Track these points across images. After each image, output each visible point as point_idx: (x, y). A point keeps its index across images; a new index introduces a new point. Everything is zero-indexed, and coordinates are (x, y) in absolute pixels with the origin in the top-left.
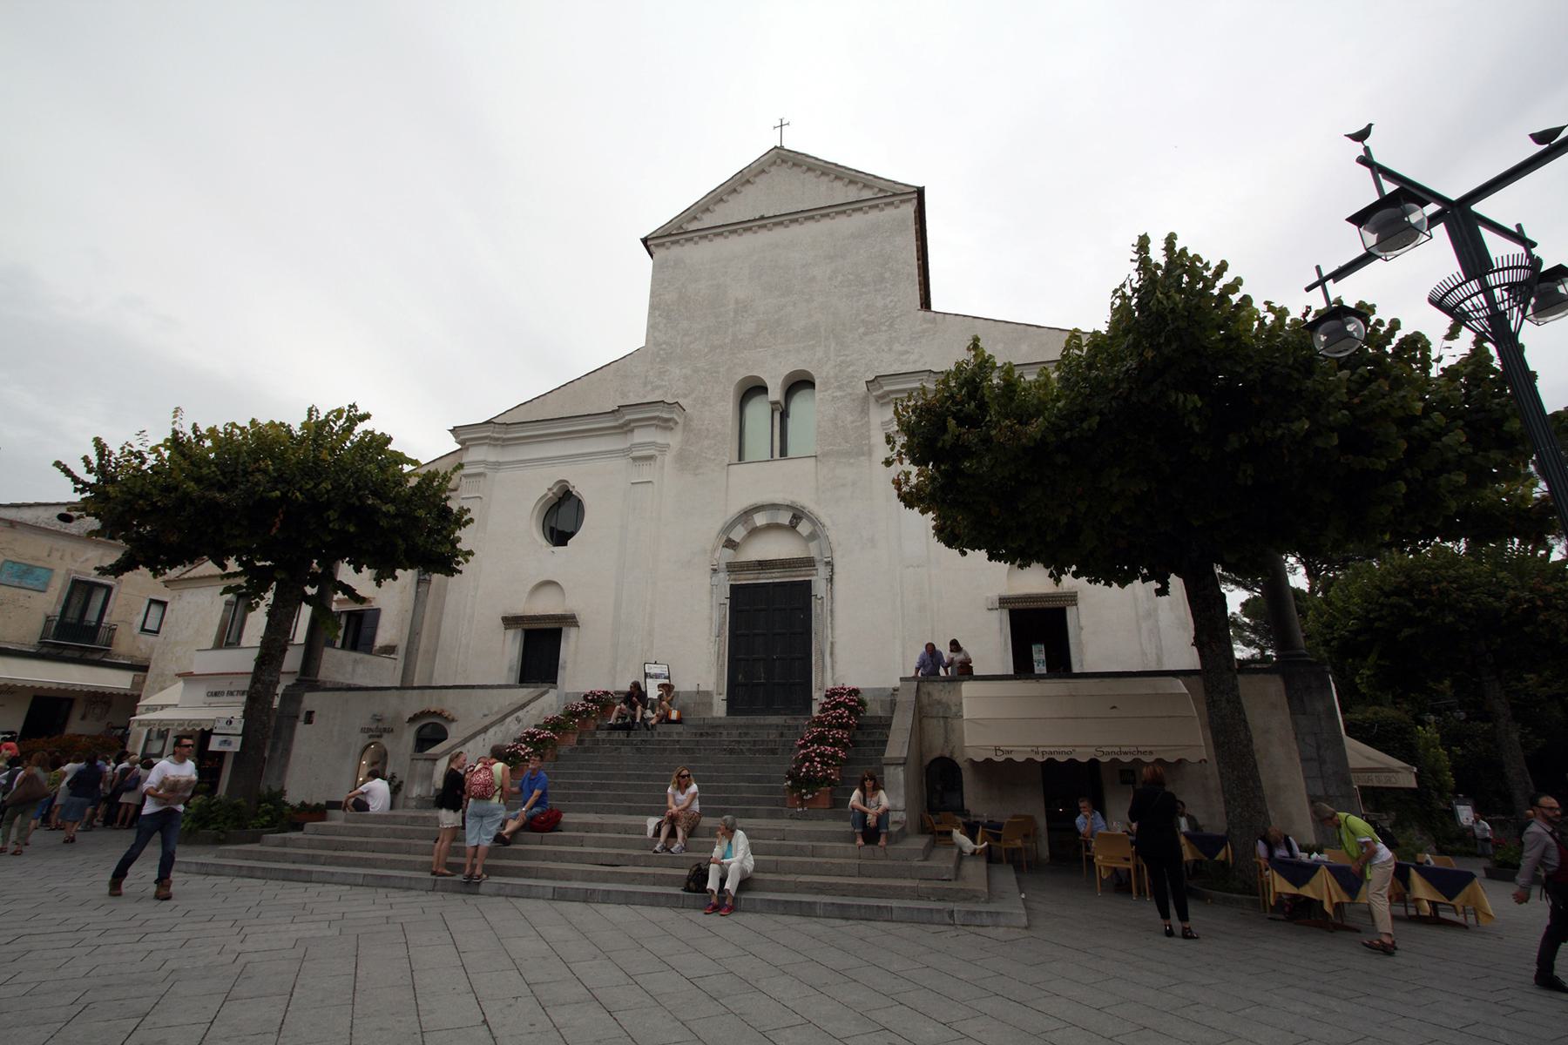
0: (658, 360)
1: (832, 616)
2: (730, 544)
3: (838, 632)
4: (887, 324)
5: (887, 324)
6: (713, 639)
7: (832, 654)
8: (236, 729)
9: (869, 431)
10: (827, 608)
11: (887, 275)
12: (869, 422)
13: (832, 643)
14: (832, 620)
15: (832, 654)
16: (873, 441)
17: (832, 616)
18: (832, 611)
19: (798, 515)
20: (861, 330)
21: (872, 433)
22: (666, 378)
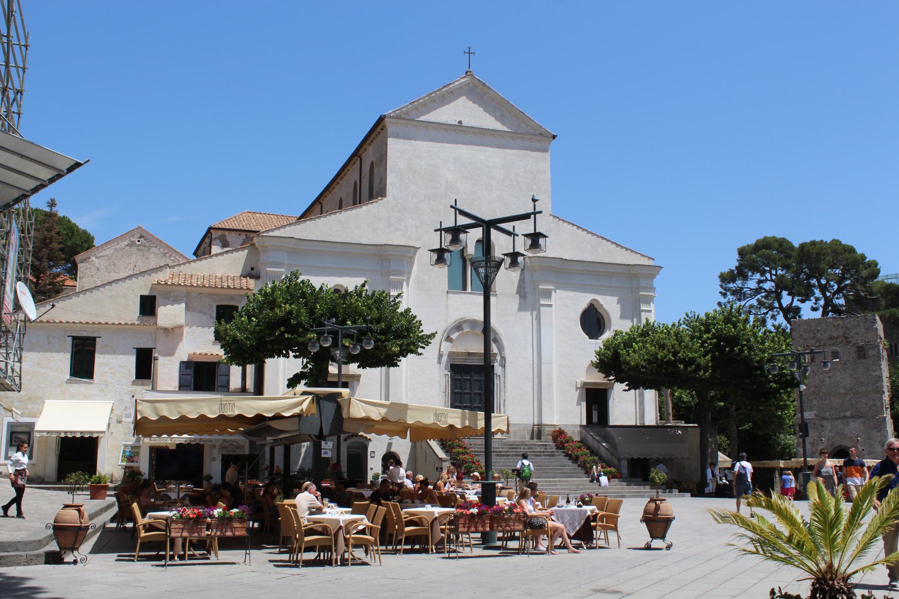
0: (397, 209)
1: (504, 385)
3: (507, 394)
6: (441, 394)
7: (504, 405)
8: (329, 446)
9: (524, 283)
10: (502, 381)
11: (534, 187)
13: (504, 400)
14: (505, 387)
15: (504, 405)
16: (527, 290)
17: (504, 385)
18: (504, 383)
21: (526, 285)
22: (403, 224)
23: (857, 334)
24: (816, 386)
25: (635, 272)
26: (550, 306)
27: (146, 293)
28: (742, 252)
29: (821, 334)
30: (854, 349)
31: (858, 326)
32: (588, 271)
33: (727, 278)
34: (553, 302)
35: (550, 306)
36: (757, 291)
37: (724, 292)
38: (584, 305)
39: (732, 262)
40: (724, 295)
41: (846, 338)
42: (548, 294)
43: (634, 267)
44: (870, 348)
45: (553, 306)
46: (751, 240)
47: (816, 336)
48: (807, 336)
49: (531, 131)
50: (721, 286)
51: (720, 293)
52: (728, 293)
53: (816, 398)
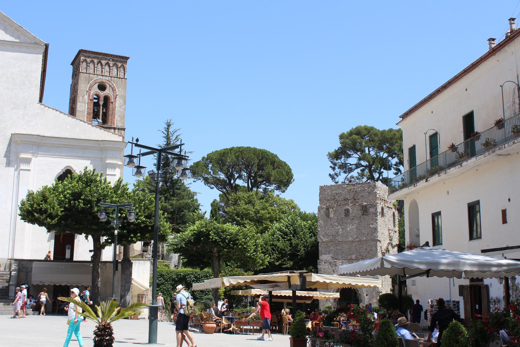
4: (23, 106)
5: (23, 106)
11: (27, 82)
12: (10, 150)
20: (12, 106)
23: (362, 196)
24: (333, 236)
25: (103, 146)
26: (29, 170)
28: (342, 137)
29: (339, 196)
30: (360, 208)
31: (364, 190)
32: (65, 145)
33: (336, 156)
34: (31, 167)
35: (29, 170)
36: (358, 166)
37: (333, 166)
38: (59, 170)
39: (336, 145)
40: (334, 169)
41: (355, 199)
43: (102, 142)
44: (371, 207)
45: (32, 171)
46: (346, 130)
47: (335, 198)
48: (329, 198)
49: (29, 40)
50: (332, 162)
51: (331, 167)
52: (336, 167)
53: (333, 245)
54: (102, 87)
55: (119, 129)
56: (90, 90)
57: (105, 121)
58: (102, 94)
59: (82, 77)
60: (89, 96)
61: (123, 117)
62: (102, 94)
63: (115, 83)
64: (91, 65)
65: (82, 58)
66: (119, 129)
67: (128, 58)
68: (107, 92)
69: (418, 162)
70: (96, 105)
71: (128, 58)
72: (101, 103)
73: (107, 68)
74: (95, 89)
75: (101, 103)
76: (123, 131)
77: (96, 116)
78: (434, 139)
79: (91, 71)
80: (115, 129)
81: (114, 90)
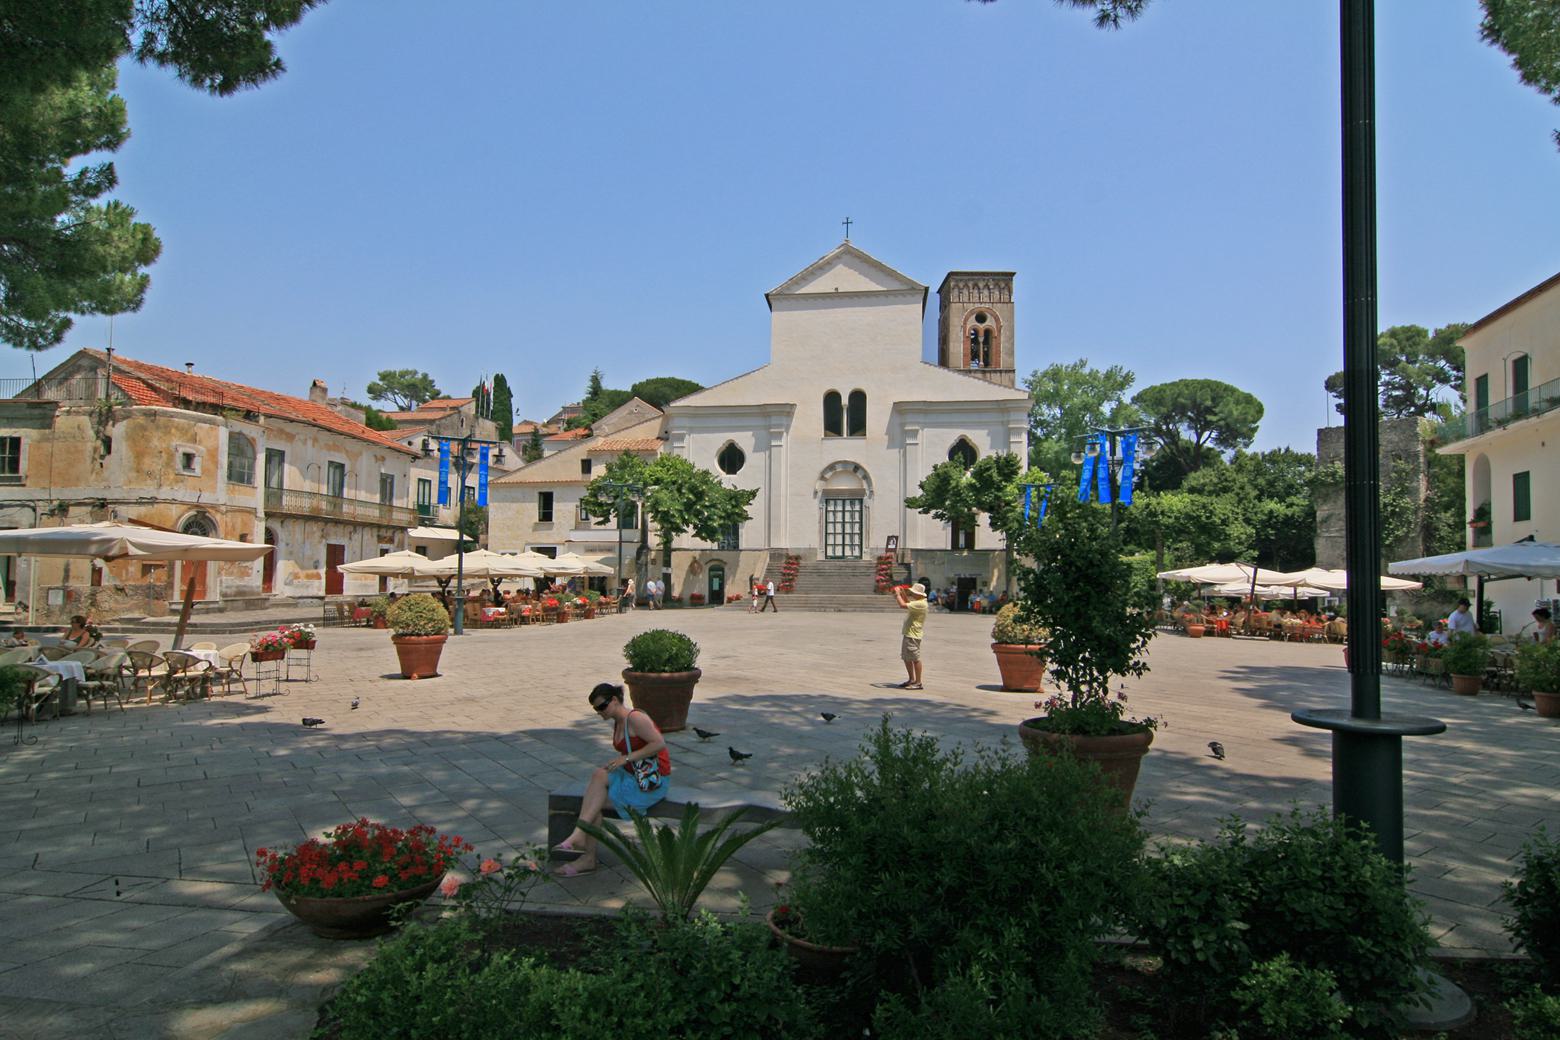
2: (822, 478)
19: (857, 468)
27: (585, 457)
34: (918, 440)
42: (914, 434)
54: (981, 318)
55: (1006, 371)
56: (965, 324)
57: (987, 364)
58: (982, 327)
59: (955, 308)
60: (965, 332)
61: (1011, 353)
62: (982, 327)
63: (998, 309)
64: (965, 292)
65: (952, 284)
66: (1006, 371)
67: (1014, 274)
68: (990, 323)
69: (1492, 400)
70: (975, 341)
71: (1014, 274)
72: (981, 339)
73: (986, 292)
74: (972, 322)
75: (981, 339)
76: (1011, 374)
77: (975, 356)
78: (1521, 367)
79: (966, 299)
80: (1001, 372)
81: (997, 319)
